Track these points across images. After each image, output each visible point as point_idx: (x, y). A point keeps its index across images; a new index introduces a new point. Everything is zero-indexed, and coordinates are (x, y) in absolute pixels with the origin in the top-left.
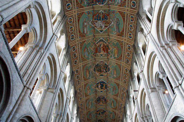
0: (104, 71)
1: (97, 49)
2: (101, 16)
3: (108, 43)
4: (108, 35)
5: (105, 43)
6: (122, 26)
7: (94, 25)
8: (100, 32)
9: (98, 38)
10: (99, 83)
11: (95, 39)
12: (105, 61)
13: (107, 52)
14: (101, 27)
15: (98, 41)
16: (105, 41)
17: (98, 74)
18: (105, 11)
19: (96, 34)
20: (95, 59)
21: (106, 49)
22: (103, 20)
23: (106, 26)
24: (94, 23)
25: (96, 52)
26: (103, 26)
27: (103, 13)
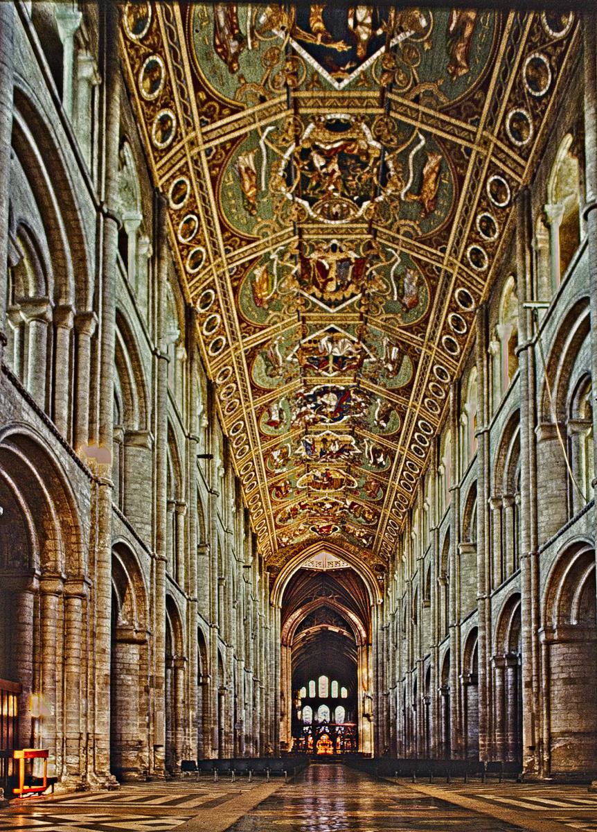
0: (319, 161)
1: (357, 275)
2: (331, 364)
3: (302, 295)
4: (304, 319)
5: (320, 296)
6: (255, 372)
7: (359, 346)
8: (336, 328)
9: (348, 312)
10: (360, 52)
11: (362, 309)
12: (314, 221)
13: (305, 262)
14: (331, 340)
15: (349, 302)
16: (315, 300)
17: (369, 140)
18: (319, 375)
19: (358, 322)
20: (371, 230)
21: (312, 275)
22: (327, 359)
23: (315, 342)
24: (357, 349)
25: (360, 263)
26: (324, 341)
27: (327, 370)
